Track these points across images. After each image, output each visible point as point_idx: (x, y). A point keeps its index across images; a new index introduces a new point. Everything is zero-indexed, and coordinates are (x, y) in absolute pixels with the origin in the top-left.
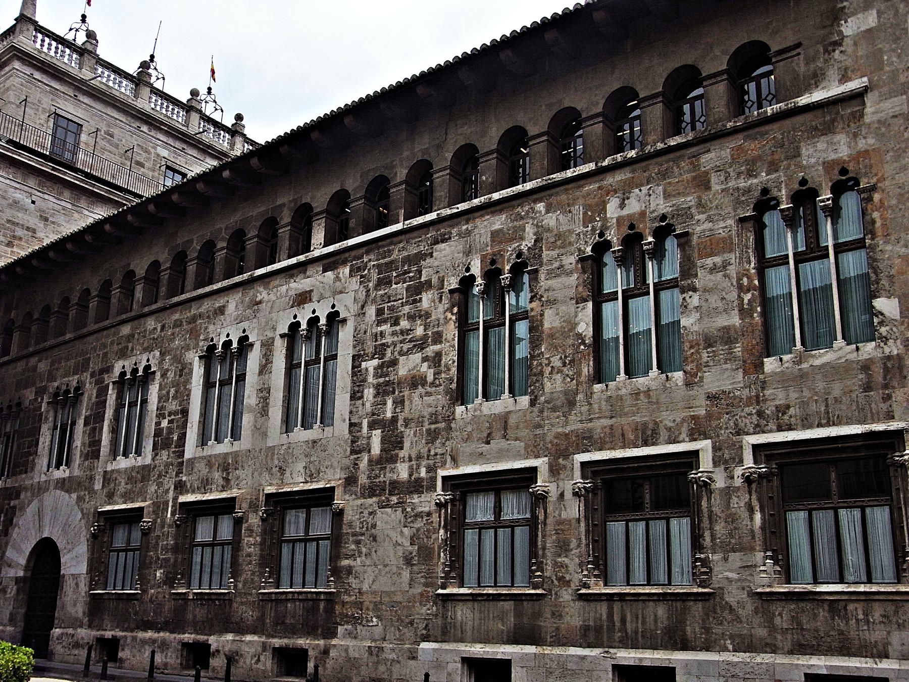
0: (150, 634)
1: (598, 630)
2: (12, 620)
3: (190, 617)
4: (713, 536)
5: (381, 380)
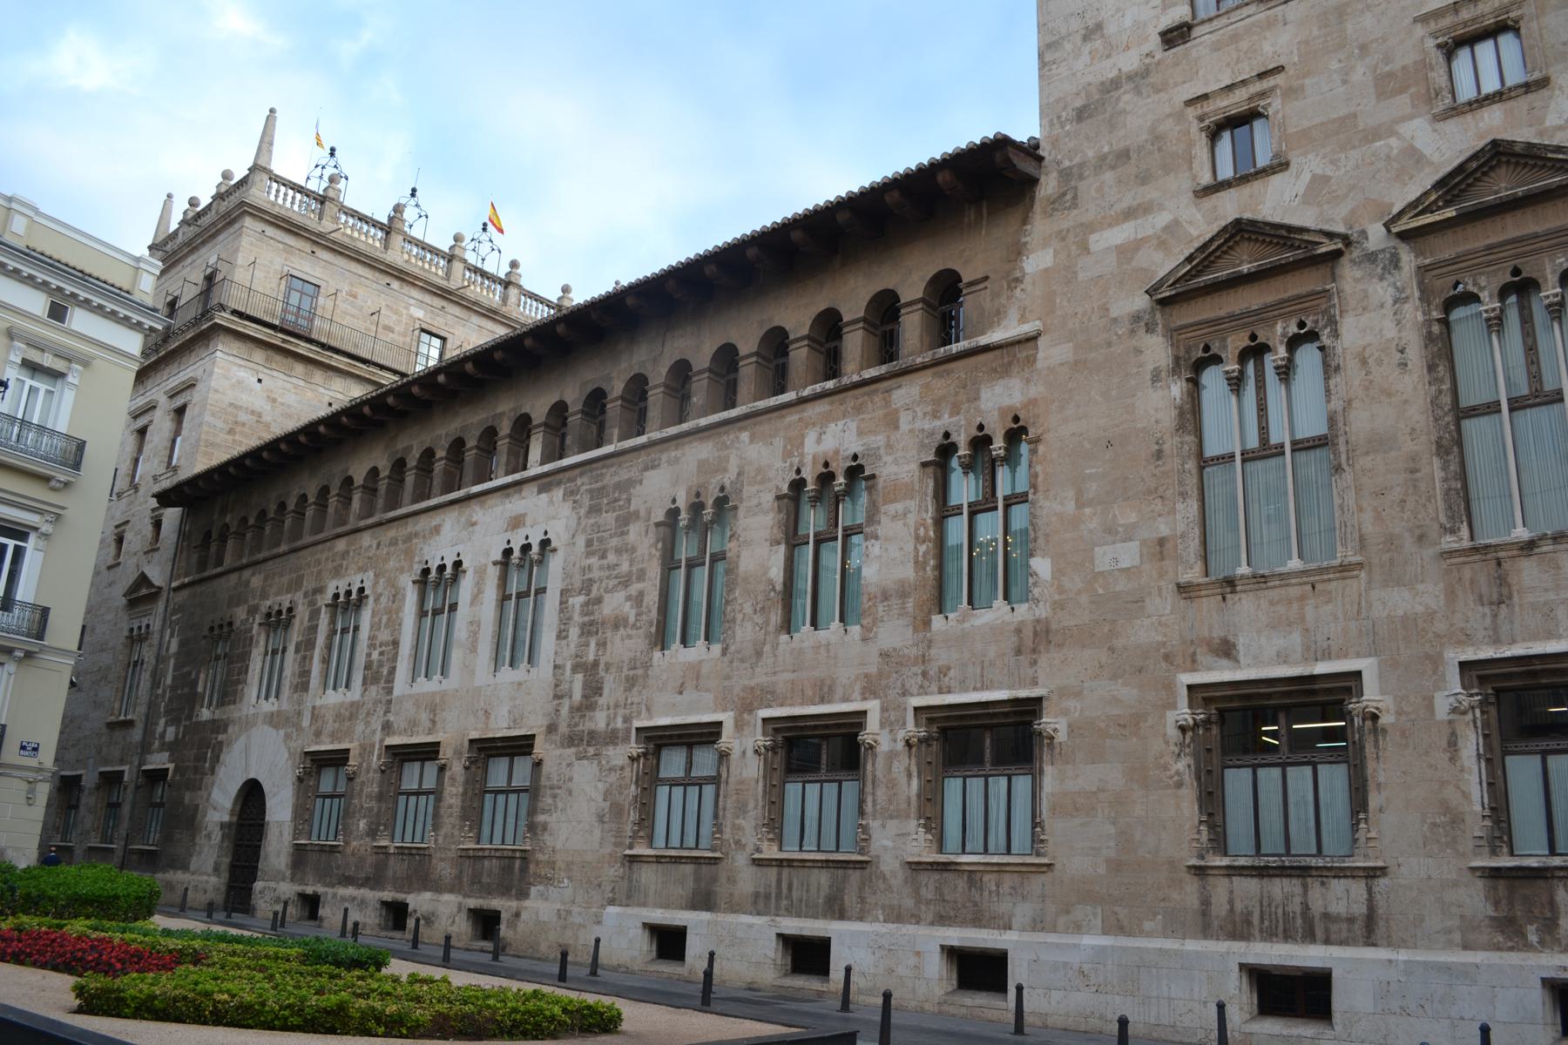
0: (350, 891)
1: (767, 897)
2: (216, 869)
3: (390, 873)
4: (874, 801)
5: (586, 619)
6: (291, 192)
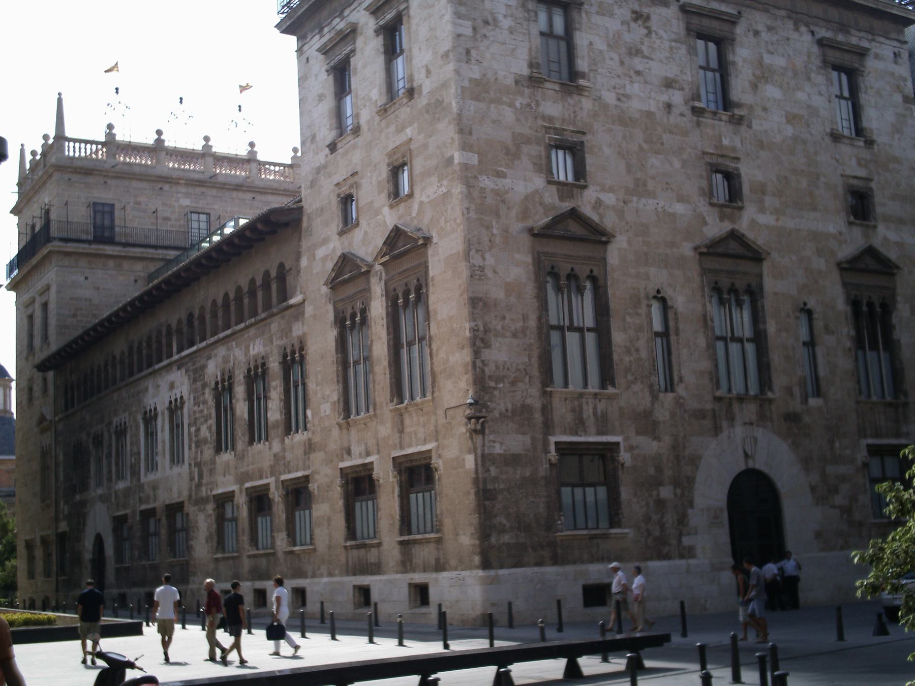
6: (83, 145)
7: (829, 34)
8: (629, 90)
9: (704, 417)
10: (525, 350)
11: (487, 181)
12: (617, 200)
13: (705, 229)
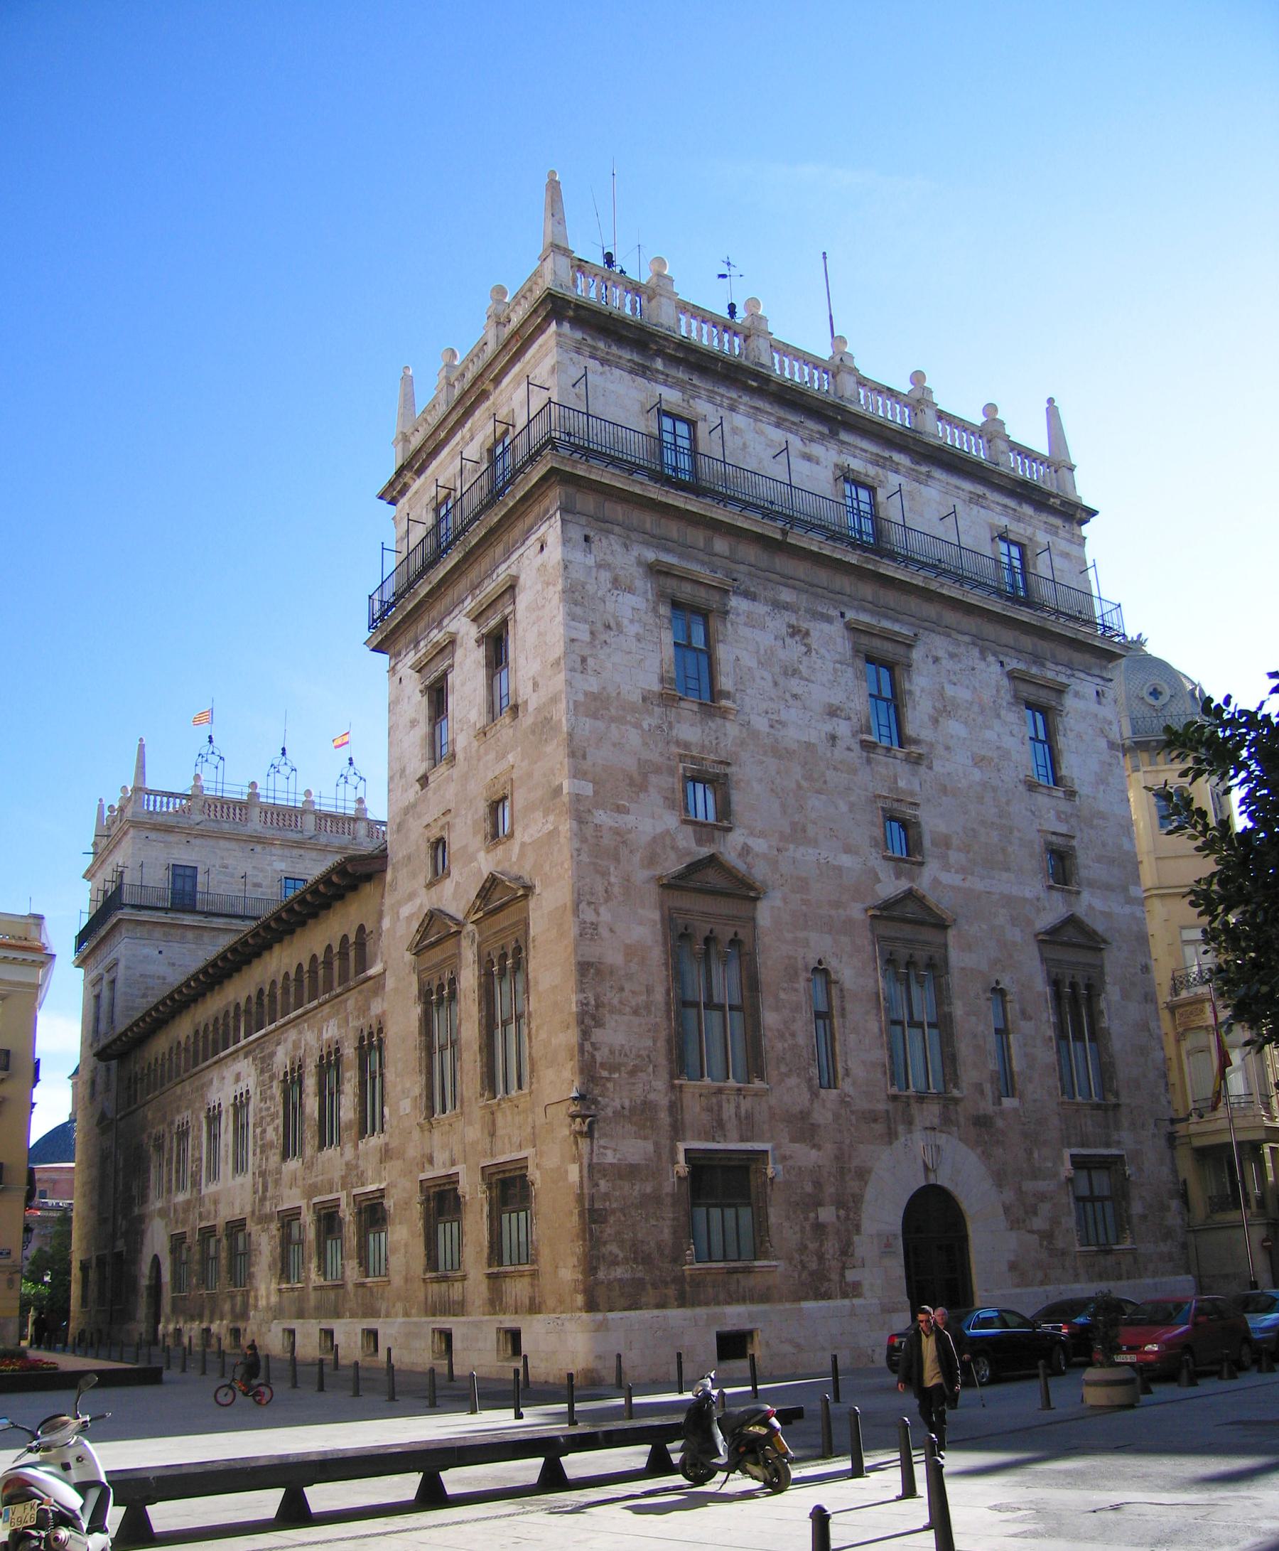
6: (165, 799)
7: (1021, 666)
8: (784, 716)
9: (875, 1120)
10: (649, 1031)
11: (604, 817)
12: (770, 847)
13: (878, 887)
